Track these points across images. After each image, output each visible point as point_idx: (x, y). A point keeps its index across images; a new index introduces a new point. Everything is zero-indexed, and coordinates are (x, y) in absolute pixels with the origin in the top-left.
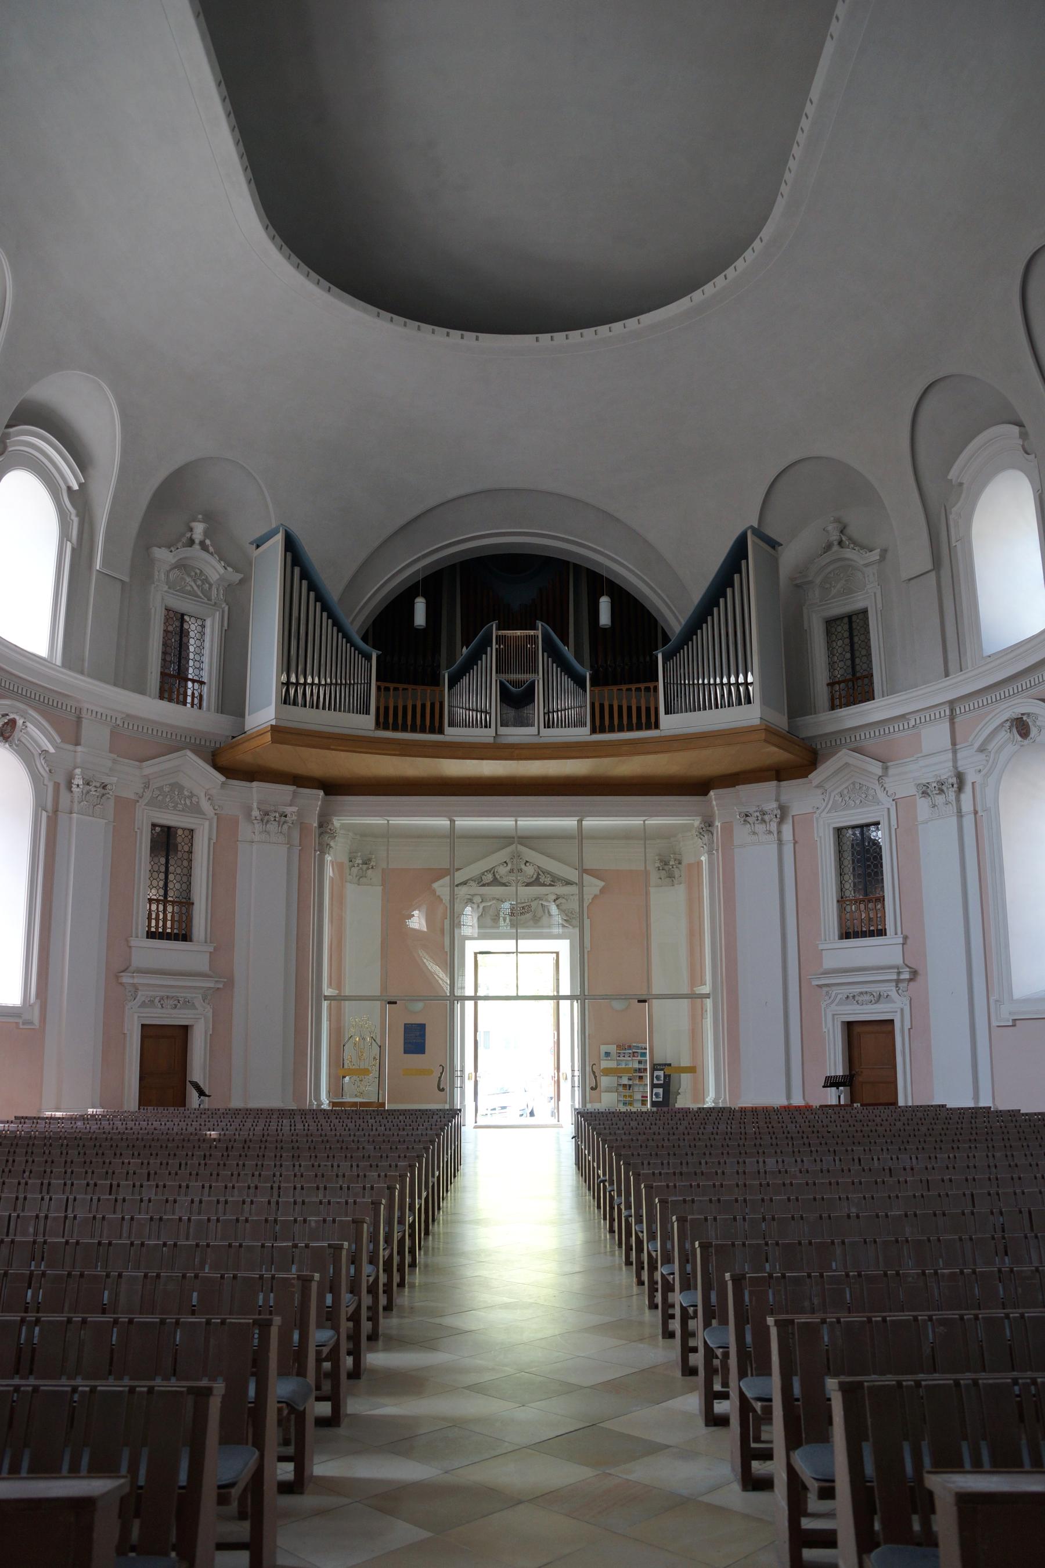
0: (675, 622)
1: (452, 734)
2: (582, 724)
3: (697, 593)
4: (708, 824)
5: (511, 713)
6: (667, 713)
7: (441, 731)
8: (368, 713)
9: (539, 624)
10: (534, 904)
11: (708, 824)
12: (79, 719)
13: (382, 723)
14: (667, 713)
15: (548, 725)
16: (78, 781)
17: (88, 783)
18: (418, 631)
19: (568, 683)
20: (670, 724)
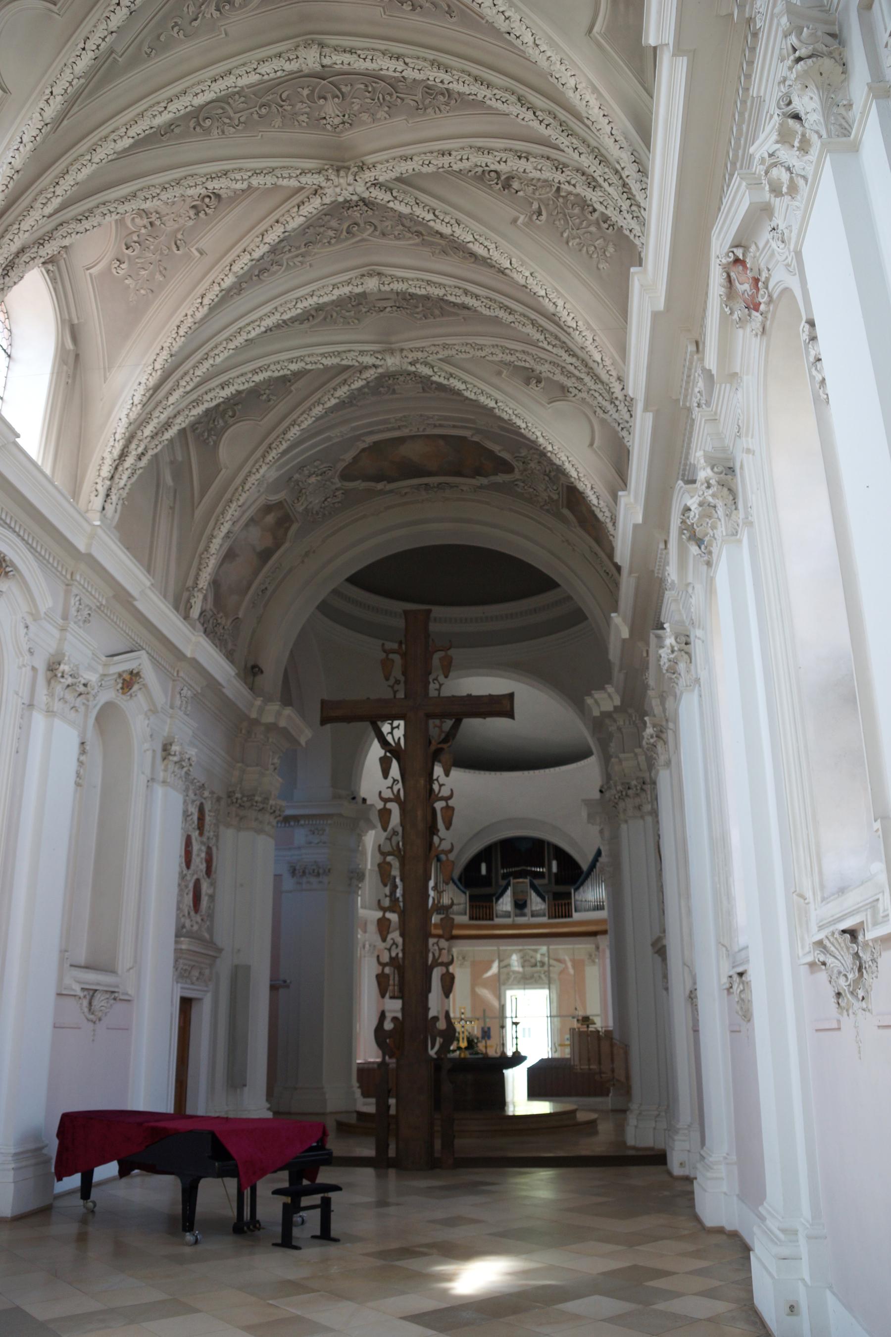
0: (585, 866)
1: (498, 921)
2: (544, 915)
3: (590, 858)
4: (598, 948)
5: (518, 911)
6: (576, 911)
7: (492, 919)
8: (465, 914)
9: (529, 878)
10: (536, 975)
11: (598, 948)
12: (366, 924)
13: (471, 918)
14: (576, 911)
15: (533, 916)
16: (367, 946)
17: (370, 946)
18: (483, 876)
19: (539, 900)
20: (576, 916)
